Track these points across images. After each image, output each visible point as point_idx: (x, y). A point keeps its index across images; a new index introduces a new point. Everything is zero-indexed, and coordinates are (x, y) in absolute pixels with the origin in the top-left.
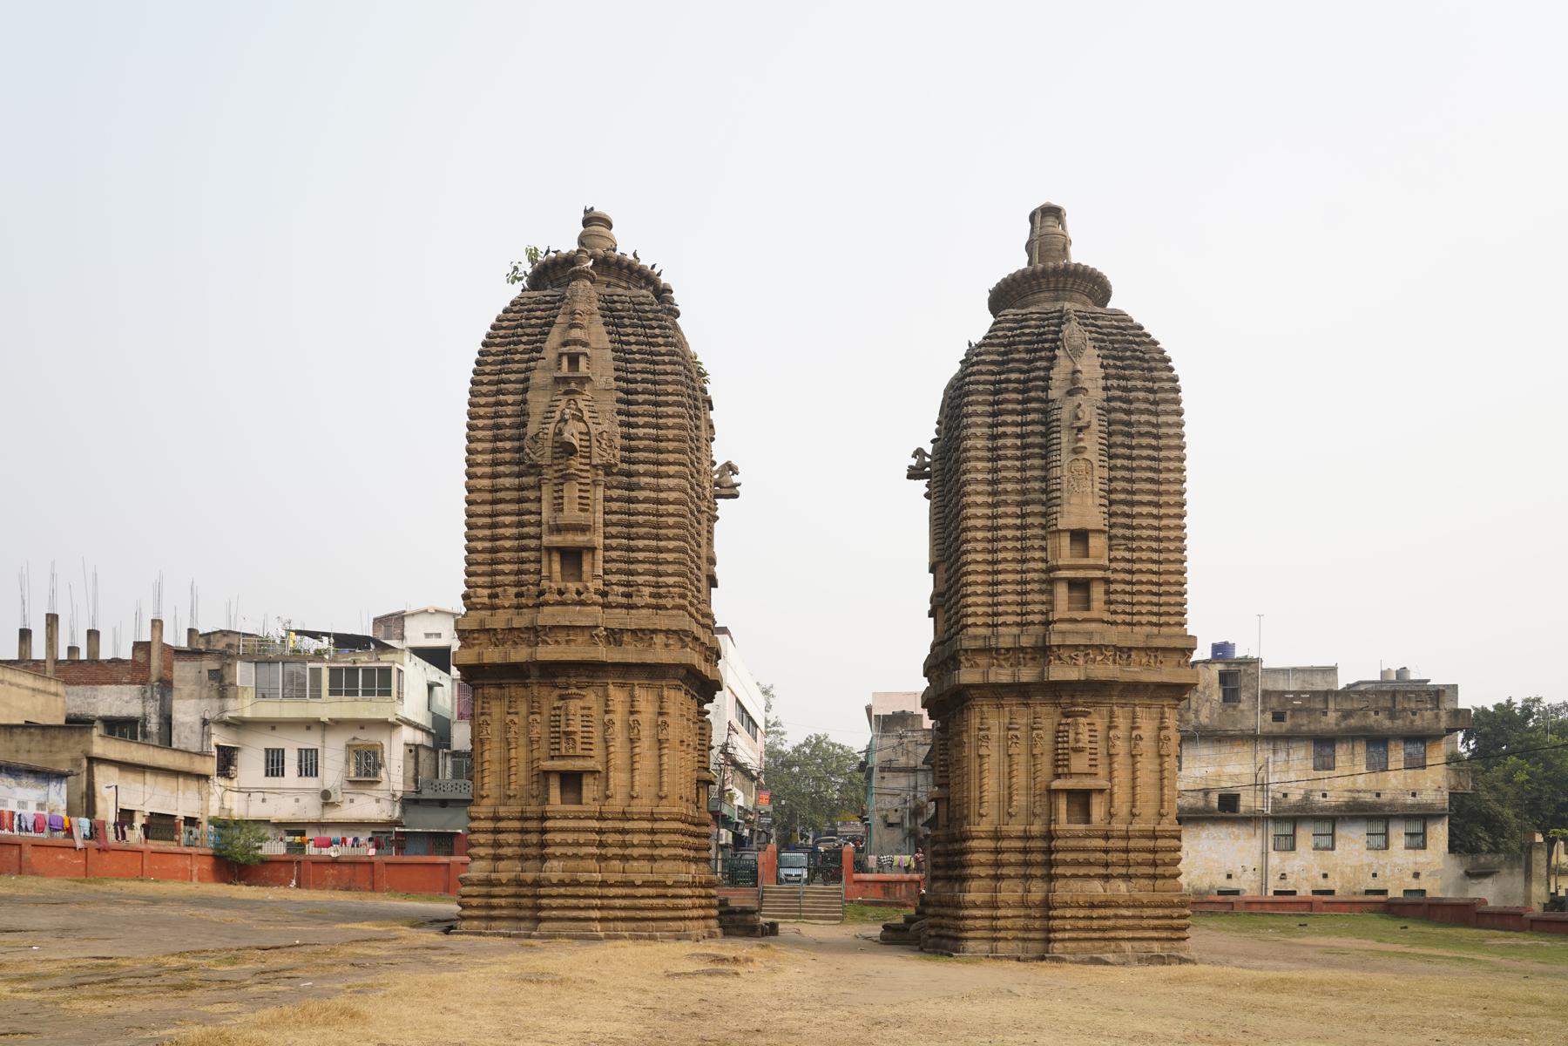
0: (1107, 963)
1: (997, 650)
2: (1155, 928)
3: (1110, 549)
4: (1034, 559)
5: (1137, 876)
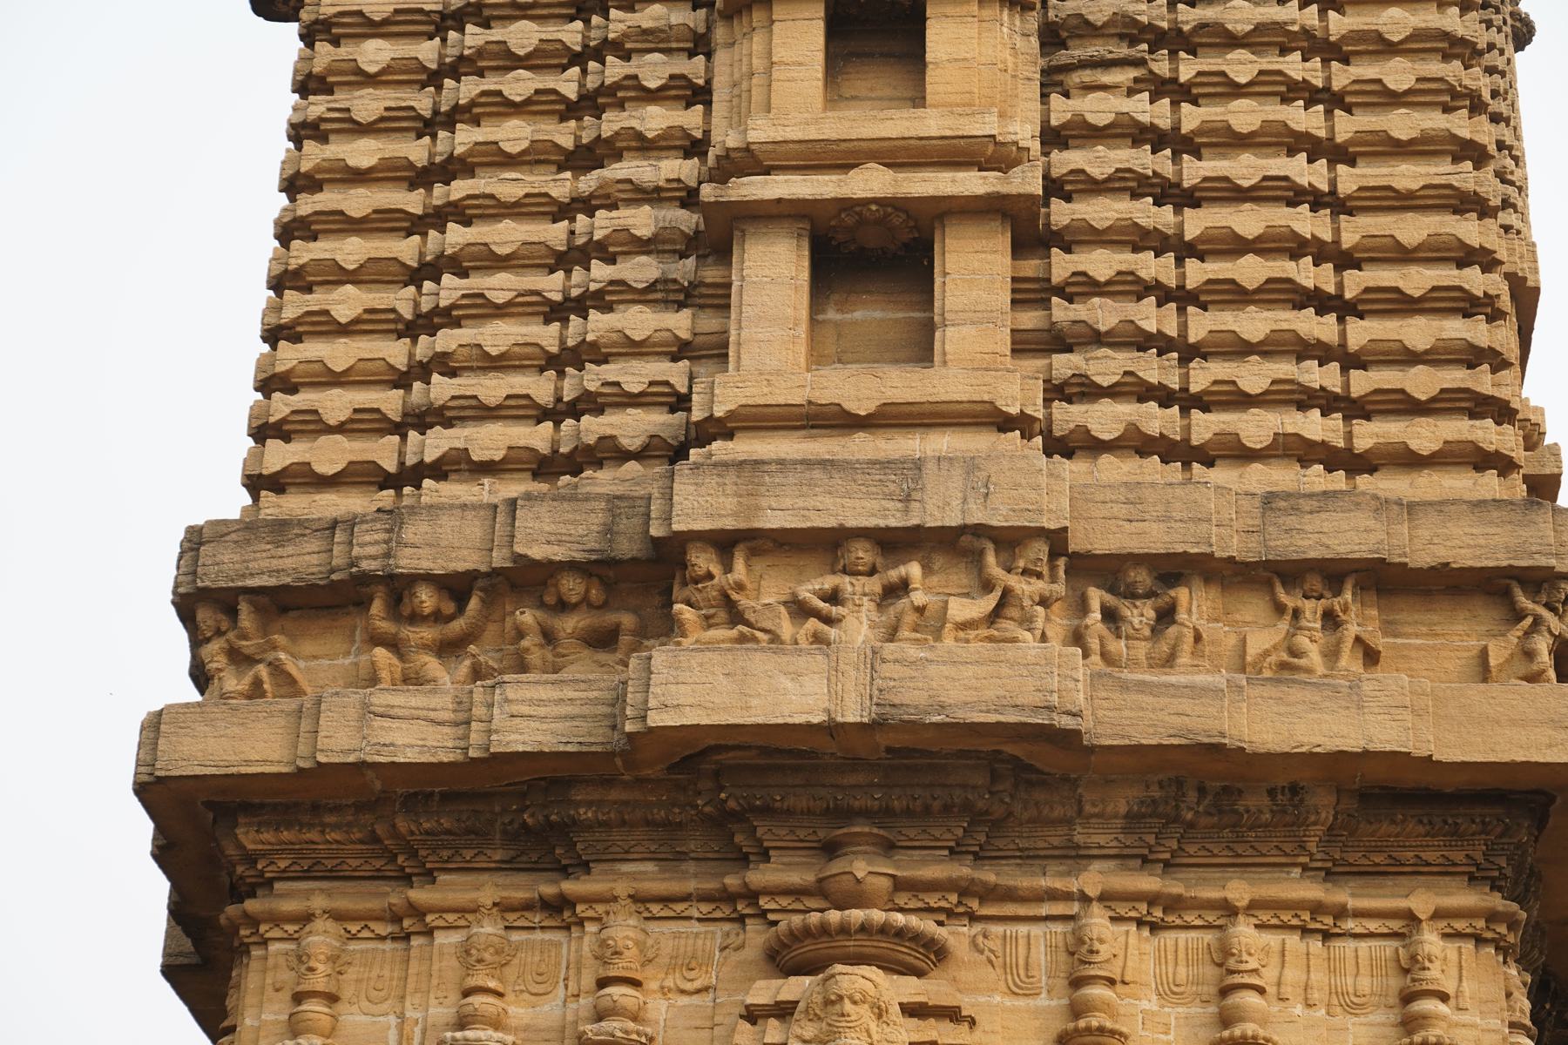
1: (398, 587)
3: (1052, 81)
4: (645, 146)
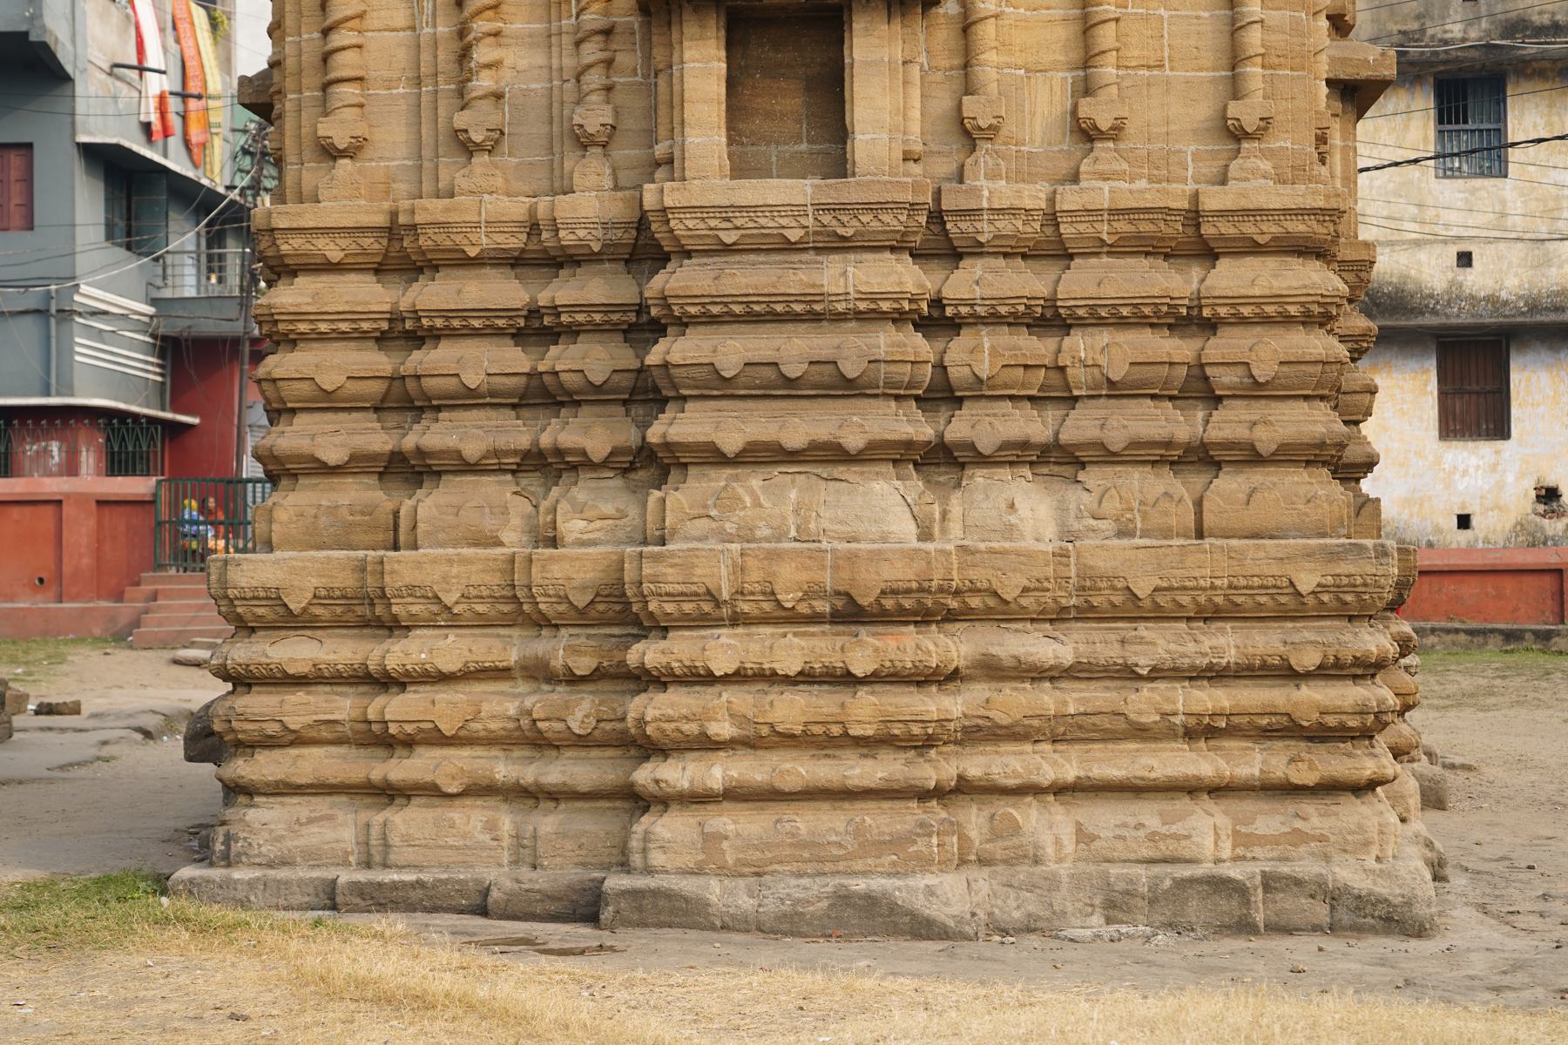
0: (923, 929)
2: (1202, 731)
5: (1109, 457)
